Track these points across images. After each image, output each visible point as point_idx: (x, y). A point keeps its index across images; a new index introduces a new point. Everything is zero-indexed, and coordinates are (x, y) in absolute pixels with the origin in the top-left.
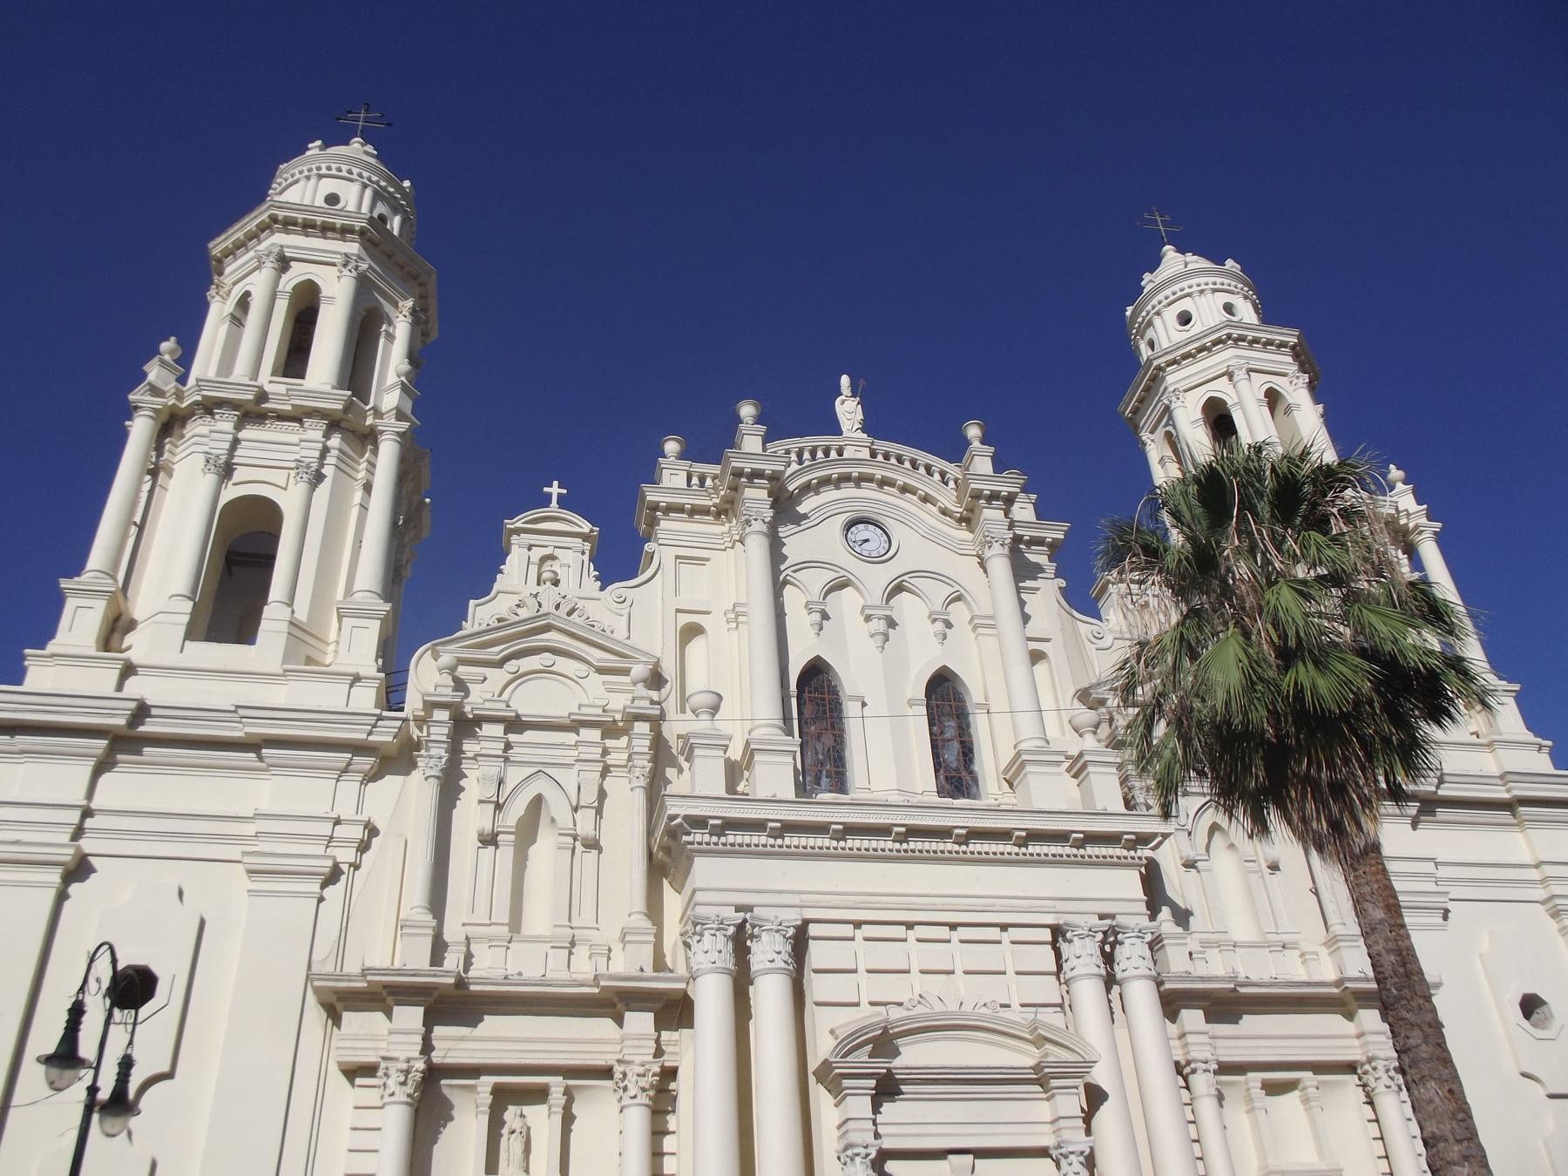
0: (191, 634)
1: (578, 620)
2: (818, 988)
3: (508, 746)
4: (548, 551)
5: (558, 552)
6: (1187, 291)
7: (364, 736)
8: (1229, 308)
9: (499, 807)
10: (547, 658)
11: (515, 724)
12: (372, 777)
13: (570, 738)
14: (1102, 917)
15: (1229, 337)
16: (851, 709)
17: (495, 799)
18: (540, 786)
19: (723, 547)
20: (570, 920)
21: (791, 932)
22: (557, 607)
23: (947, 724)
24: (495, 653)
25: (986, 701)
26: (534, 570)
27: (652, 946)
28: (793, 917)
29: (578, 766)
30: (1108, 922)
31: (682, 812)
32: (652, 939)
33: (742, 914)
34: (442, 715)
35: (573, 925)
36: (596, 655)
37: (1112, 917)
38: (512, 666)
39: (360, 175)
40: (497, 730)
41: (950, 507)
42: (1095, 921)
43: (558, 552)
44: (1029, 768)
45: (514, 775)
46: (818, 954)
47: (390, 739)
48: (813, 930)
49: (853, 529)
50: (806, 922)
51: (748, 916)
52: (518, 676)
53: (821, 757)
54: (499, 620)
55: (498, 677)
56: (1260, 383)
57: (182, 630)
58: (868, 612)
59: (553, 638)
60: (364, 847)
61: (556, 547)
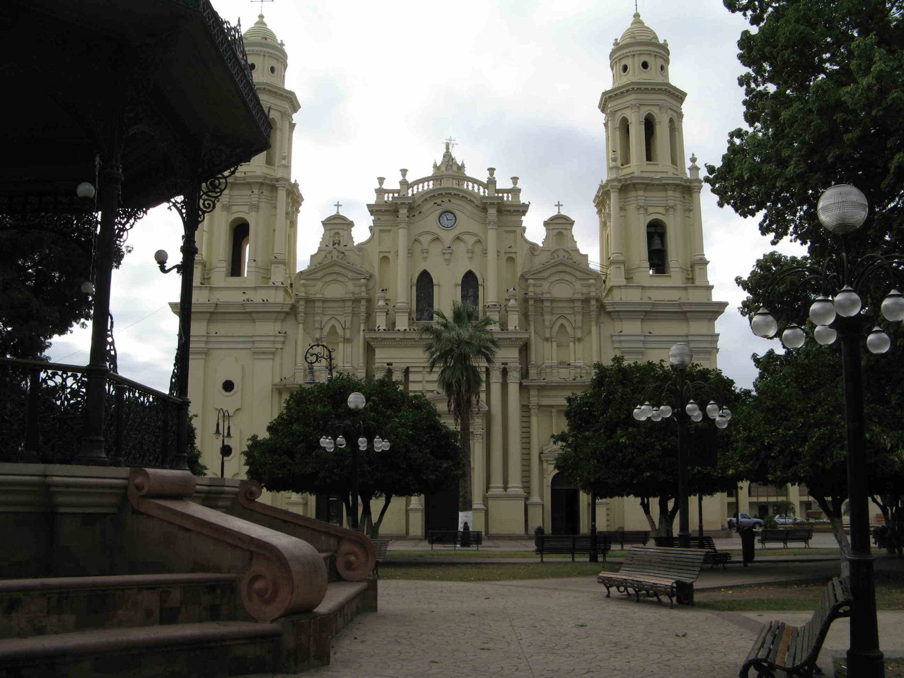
0: (227, 276)
1: (345, 262)
4: (337, 231)
5: (340, 231)
6: (628, 54)
8: (645, 65)
10: (335, 276)
11: (325, 301)
12: (283, 320)
13: (341, 304)
14: (503, 364)
15: (633, 89)
16: (435, 288)
18: (333, 322)
20: (343, 364)
21: (403, 370)
24: (319, 275)
28: (404, 366)
29: (345, 315)
32: (365, 371)
36: (350, 274)
37: (507, 364)
38: (325, 280)
41: (479, 205)
43: (340, 231)
45: (326, 319)
46: (412, 377)
47: (287, 310)
48: (411, 370)
50: (408, 368)
54: (319, 263)
55: (320, 284)
56: (644, 111)
58: (444, 251)
59: (336, 269)
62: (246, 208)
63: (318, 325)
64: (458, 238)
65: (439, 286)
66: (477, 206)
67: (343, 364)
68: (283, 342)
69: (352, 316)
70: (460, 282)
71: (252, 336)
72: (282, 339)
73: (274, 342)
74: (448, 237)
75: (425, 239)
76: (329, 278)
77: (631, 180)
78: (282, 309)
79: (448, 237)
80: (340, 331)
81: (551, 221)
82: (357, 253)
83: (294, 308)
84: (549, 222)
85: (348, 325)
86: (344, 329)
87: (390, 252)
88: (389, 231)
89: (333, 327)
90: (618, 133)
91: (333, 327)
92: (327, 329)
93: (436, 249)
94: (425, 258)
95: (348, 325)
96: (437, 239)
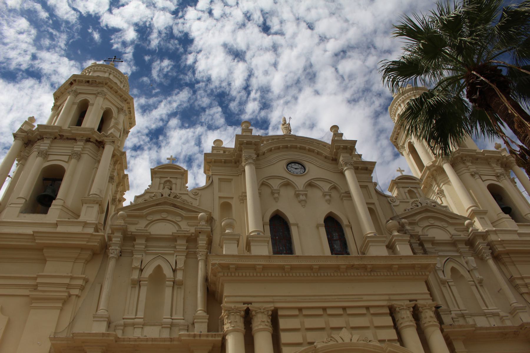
2: (285, 337)
3: (146, 247)
4: (169, 179)
5: (172, 180)
7: (85, 243)
9: (141, 270)
10: (164, 215)
11: (149, 238)
16: (294, 231)
17: (140, 267)
18: (159, 262)
19: (238, 175)
20: (171, 315)
22: (169, 195)
23: (334, 234)
25: (350, 223)
26: (162, 186)
27: (206, 324)
28: (271, 306)
30: (414, 302)
31: (217, 262)
33: (246, 305)
34: (119, 234)
35: (172, 318)
38: (150, 218)
39: (108, 70)
40: (143, 241)
42: (408, 302)
44: (370, 244)
45: (149, 258)
46: (283, 323)
48: (280, 313)
49: (290, 165)
51: (249, 305)
52: (152, 222)
53: (281, 248)
57: (18, 210)
60: (82, 288)
61: (170, 178)
62: (66, 158)
63: (136, 264)
64: (310, 185)
65: (297, 225)
66: (326, 157)
67: (171, 315)
68: (82, 288)
69: (187, 257)
70: (322, 222)
71: (35, 278)
72: (80, 282)
73: (69, 286)
74: (300, 182)
75: (275, 184)
76: (158, 217)
77: (459, 153)
78: (88, 242)
79: (300, 182)
80: (168, 272)
81: (399, 180)
82: (193, 196)
83: (105, 247)
84: (397, 181)
85: (180, 265)
86: (174, 271)
87: (232, 198)
88: (230, 181)
89: (159, 268)
90: (411, 156)
91: (159, 268)
92: (148, 272)
93: (287, 194)
94: (276, 200)
95: (180, 265)
96: (288, 184)
